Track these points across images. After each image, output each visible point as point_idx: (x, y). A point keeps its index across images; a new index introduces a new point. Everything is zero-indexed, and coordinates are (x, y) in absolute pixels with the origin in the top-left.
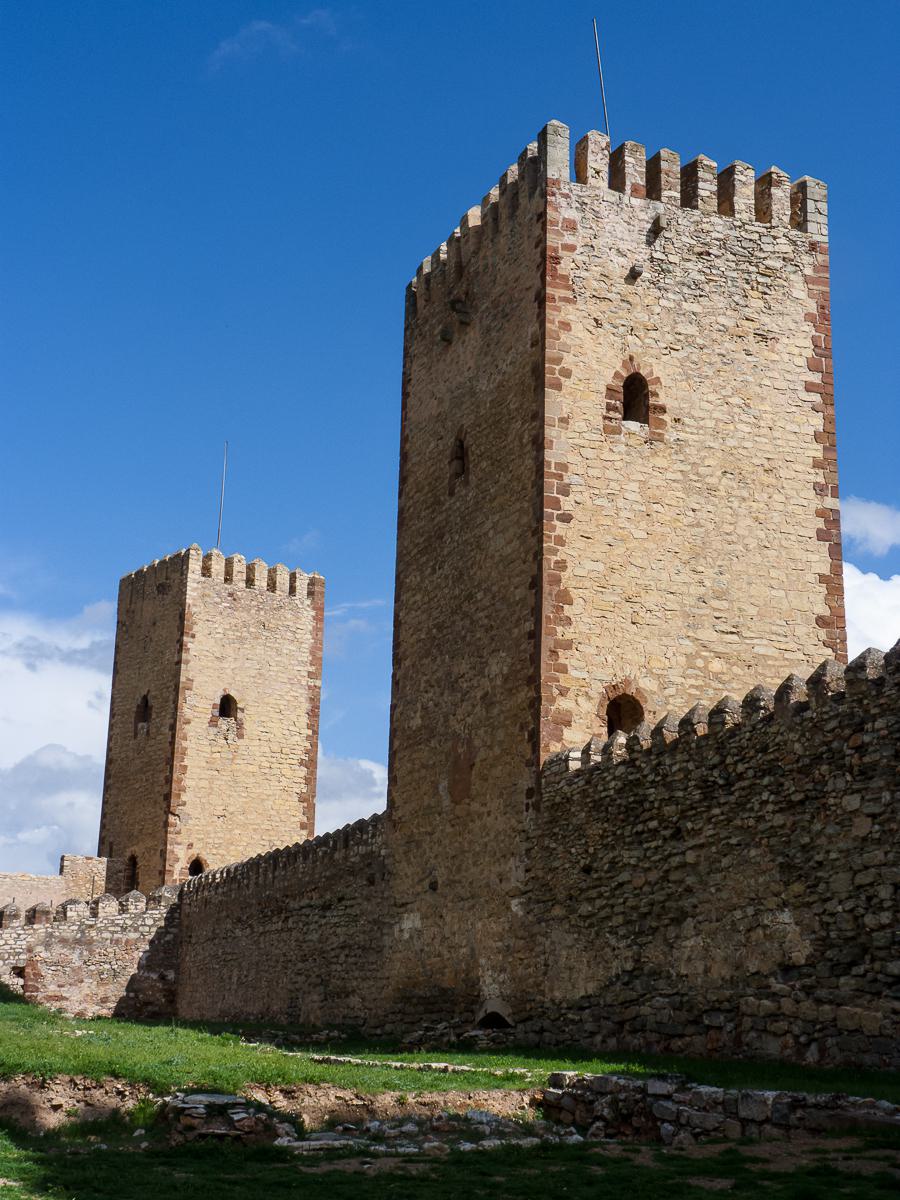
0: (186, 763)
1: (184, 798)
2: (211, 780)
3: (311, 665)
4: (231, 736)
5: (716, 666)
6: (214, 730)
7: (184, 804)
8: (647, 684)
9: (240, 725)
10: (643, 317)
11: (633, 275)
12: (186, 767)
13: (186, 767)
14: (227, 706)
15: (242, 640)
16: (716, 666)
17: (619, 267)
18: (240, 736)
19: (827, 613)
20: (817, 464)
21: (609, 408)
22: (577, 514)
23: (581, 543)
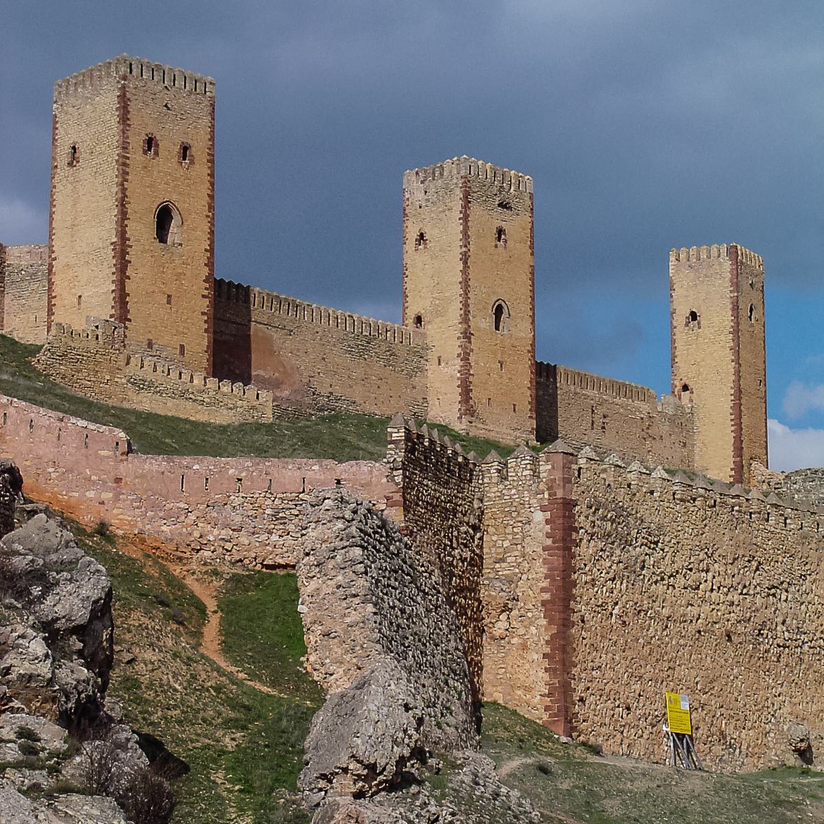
0: (676, 345)
1: (676, 360)
2: (688, 349)
3: (731, 286)
4: (695, 329)
5: (437, 302)
6: (688, 328)
7: (677, 363)
8: (423, 311)
9: (699, 323)
10: (423, 217)
11: (420, 207)
12: (676, 347)
13: (676, 347)
14: (694, 316)
15: (696, 285)
16: (437, 302)
17: (418, 203)
18: (699, 328)
19: (461, 280)
20: (461, 240)
21: (416, 244)
22: (409, 275)
23: (410, 281)
